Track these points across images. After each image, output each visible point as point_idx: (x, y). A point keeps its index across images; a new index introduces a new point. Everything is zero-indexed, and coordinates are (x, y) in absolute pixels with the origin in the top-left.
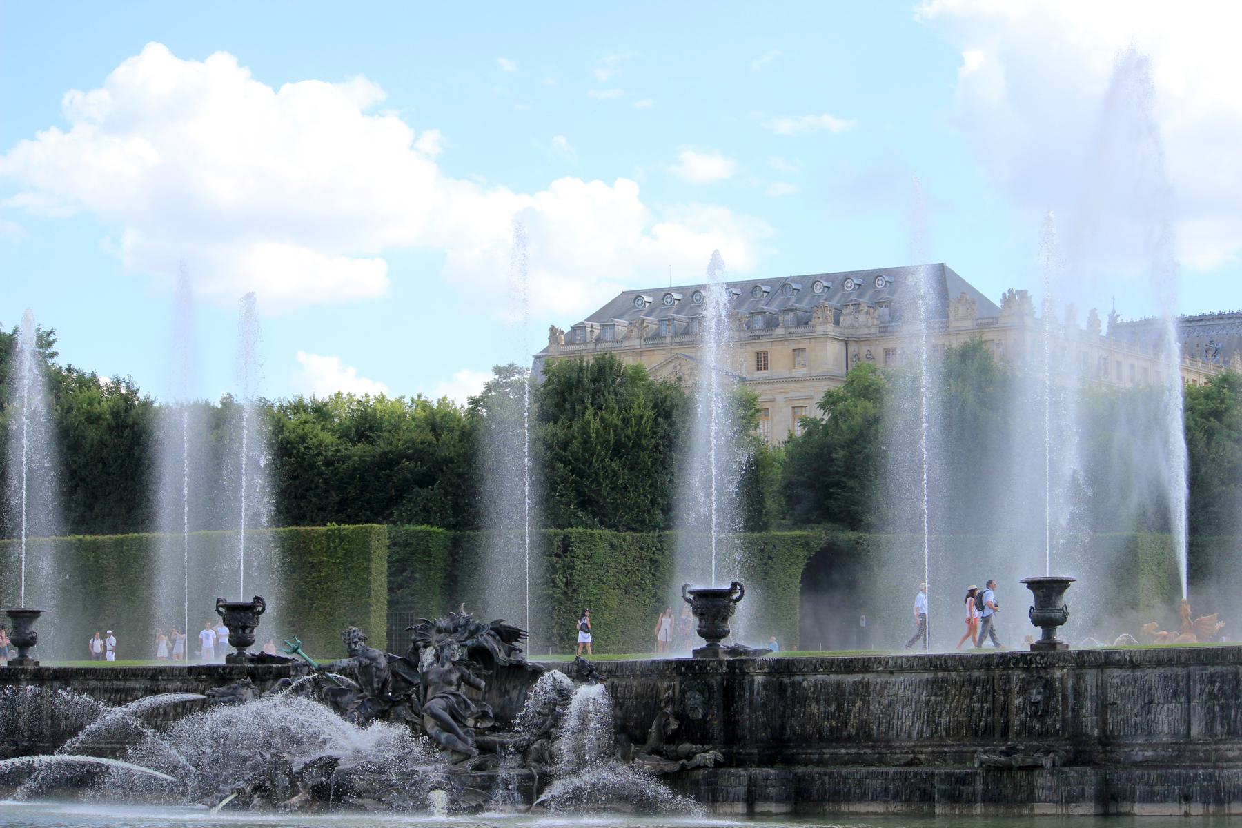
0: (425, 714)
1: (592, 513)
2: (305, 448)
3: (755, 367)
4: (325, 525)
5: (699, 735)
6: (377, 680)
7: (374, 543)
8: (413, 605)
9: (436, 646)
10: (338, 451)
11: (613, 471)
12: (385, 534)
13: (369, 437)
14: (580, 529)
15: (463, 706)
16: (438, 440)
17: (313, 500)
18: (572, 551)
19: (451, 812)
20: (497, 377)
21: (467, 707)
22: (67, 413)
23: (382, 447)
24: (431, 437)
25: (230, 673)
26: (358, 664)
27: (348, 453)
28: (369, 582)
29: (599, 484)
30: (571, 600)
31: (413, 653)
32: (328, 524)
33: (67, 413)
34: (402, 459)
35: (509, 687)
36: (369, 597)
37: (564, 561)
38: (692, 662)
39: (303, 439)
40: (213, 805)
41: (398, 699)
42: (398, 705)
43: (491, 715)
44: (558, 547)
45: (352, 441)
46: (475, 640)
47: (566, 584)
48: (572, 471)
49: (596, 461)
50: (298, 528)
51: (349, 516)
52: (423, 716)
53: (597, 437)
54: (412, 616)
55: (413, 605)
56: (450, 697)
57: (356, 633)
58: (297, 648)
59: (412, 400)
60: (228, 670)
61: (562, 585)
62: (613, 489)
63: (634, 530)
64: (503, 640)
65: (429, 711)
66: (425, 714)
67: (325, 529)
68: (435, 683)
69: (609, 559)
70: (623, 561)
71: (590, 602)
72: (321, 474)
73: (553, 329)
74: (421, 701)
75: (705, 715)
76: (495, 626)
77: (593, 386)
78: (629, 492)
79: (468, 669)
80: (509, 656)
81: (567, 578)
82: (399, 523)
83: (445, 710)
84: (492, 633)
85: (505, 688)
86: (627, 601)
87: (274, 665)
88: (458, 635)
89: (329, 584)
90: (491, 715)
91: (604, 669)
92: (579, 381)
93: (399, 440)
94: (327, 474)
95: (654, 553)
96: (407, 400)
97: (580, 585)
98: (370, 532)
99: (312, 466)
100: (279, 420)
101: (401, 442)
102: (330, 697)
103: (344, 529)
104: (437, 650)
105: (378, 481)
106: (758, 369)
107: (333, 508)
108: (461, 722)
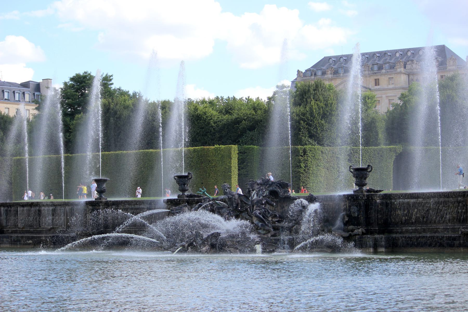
0: (253, 216)
1: (314, 140)
2: (206, 117)
3: (374, 85)
4: (214, 146)
5: (356, 223)
7: (233, 152)
8: (247, 175)
9: (257, 190)
10: (219, 118)
11: (322, 124)
12: (237, 149)
13: (230, 112)
14: (310, 146)
15: (267, 213)
16: (256, 113)
17: (209, 136)
18: (307, 154)
19: (263, 252)
20: (278, 89)
22: (116, 105)
23: (235, 116)
24: (253, 112)
25: (179, 202)
26: (227, 197)
27: (222, 118)
28: (231, 167)
29: (317, 129)
30: (307, 173)
31: (248, 193)
32: (215, 145)
33: (116, 105)
34: (243, 120)
35: (284, 205)
36: (231, 172)
37: (304, 158)
38: (353, 195)
39: (205, 113)
40: (173, 252)
41: (242, 210)
42: (243, 213)
43: (278, 216)
44: (302, 153)
45: (223, 114)
47: (305, 167)
48: (307, 124)
49: (316, 120)
50: (204, 147)
51: (223, 142)
52: (252, 217)
53: (316, 111)
54: (247, 180)
55: (247, 175)
58: (205, 192)
59: (246, 98)
60: (178, 200)
61: (303, 167)
62: (322, 131)
63: (330, 146)
64: (282, 188)
65: (254, 215)
66: (253, 216)
67: (214, 147)
69: (321, 157)
70: (326, 158)
71: (314, 173)
72: (212, 126)
73: (298, 71)
74: (252, 211)
75: (358, 215)
77: (314, 92)
78: (328, 132)
79: (269, 199)
80: (284, 194)
81: (305, 165)
82: (242, 145)
86: (328, 173)
87: (196, 198)
89: (216, 168)
90: (278, 216)
91: (320, 198)
92: (309, 90)
93: (241, 113)
94: (214, 127)
95: (338, 155)
96: (244, 99)
97: (310, 167)
98: (231, 148)
99: (209, 123)
100: (196, 106)
101: (242, 114)
102: (217, 210)
103: (221, 147)
104: (257, 192)
105: (234, 129)
106: (376, 85)
107: (217, 139)
108: (267, 219)
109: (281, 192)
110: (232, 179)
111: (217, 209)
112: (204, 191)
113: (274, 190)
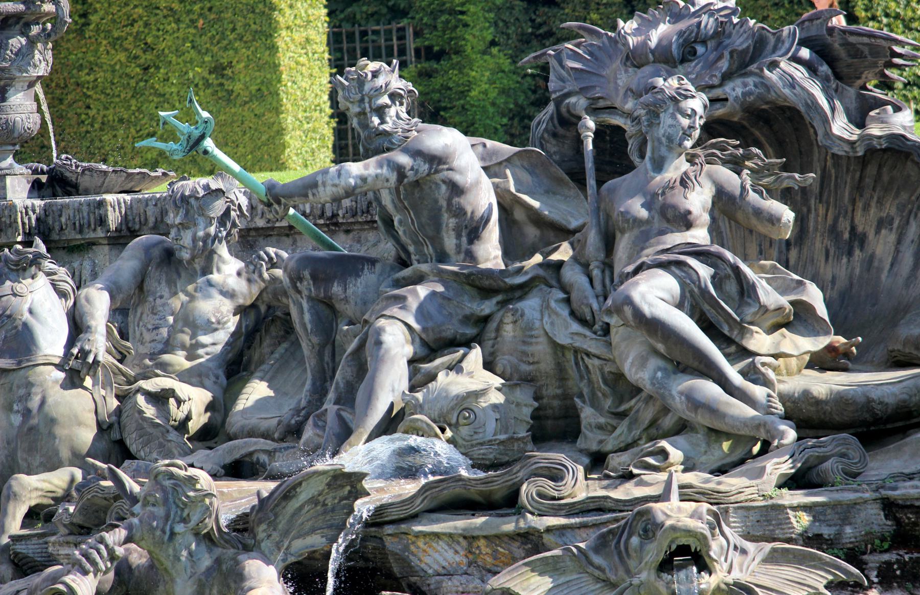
0: (613, 321)
6: (452, 222)
15: (732, 287)
21: (746, 291)
26: (393, 177)
35: (865, 222)
43: (822, 311)
46: (750, 80)
56: (692, 262)
57: (381, 81)
58: (202, 137)
64: (838, 76)
68: (638, 222)
76: (813, 32)
83: (680, 306)
84: (805, 53)
85: (853, 229)
87: (110, 198)
88: (694, 66)
90: (822, 311)
109: (833, 109)
110: (283, 39)
111: (306, 274)
112: (197, 133)
113: (772, 96)
